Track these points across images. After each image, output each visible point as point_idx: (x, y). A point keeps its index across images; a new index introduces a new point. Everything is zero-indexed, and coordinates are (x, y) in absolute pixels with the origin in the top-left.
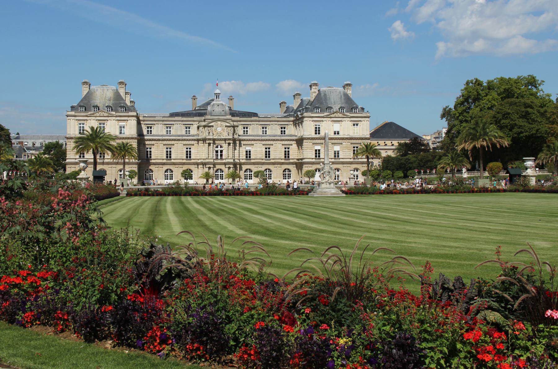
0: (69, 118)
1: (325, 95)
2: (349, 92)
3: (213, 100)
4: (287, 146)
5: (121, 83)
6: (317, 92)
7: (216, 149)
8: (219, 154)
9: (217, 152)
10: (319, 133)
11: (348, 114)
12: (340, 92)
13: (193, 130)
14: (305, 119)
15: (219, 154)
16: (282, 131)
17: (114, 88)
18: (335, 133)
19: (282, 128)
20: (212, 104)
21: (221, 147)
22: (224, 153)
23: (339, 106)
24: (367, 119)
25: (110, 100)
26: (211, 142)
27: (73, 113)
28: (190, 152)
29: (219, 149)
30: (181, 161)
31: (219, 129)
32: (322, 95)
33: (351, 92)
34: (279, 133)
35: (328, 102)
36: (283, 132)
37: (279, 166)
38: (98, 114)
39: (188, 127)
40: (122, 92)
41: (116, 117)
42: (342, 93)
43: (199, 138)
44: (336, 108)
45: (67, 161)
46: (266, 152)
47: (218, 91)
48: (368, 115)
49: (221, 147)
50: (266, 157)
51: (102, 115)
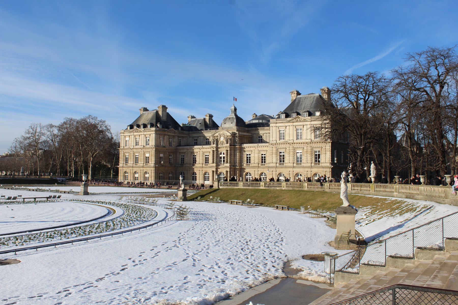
1: (299, 101)
7: (220, 156)
8: (222, 159)
9: (221, 158)
10: (284, 139)
15: (222, 159)
21: (224, 154)
22: (225, 159)
26: (215, 149)
29: (222, 156)
31: (222, 139)
32: (297, 101)
35: (299, 108)
42: (315, 98)
46: (262, 157)
49: (224, 154)
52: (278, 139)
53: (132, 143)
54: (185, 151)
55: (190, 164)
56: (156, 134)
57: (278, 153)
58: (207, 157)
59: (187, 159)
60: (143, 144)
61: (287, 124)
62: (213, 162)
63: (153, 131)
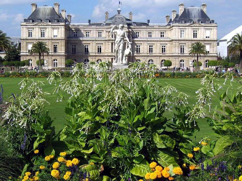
0: (22, 26)
1: (188, 11)
2: (205, 10)
3: (116, 15)
4: (164, 45)
5: (55, 4)
6: (183, 10)
11: (203, 24)
12: (198, 10)
13: (104, 34)
14: (174, 27)
16: (161, 35)
17: (51, 7)
18: (194, 37)
19: (161, 33)
20: (115, 17)
23: (197, 19)
24: (216, 28)
25: (48, 15)
27: (25, 24)
28: (100, 48)
30: (95, 54)
32: (187, 11)
33: (206, 10)
34: (160, 36)
35: (190, 16)
36: (150, 36)
37: (158, 57)
38: (40, 24)
39: (100, 33)
40: (56, 9)
41: (52, 26)
42: (200, 11)
43: (106, 39)
44: (196, 20)
45: (21, 54)
46: (150, 48)
47: (119, 9)
48: (216, 25)
50: (150, 52)
51: (43, 25)
52: (180, 37)
53: (37, 34)
54: (77, 42)
55: (83, 53)
56: (65, 29)
57: (180, 47)
58: (99, 47)
59: (78, 48)
60: (50, 36)
61: (187, 28)
62: (112, 51)
63: (62, 25)
